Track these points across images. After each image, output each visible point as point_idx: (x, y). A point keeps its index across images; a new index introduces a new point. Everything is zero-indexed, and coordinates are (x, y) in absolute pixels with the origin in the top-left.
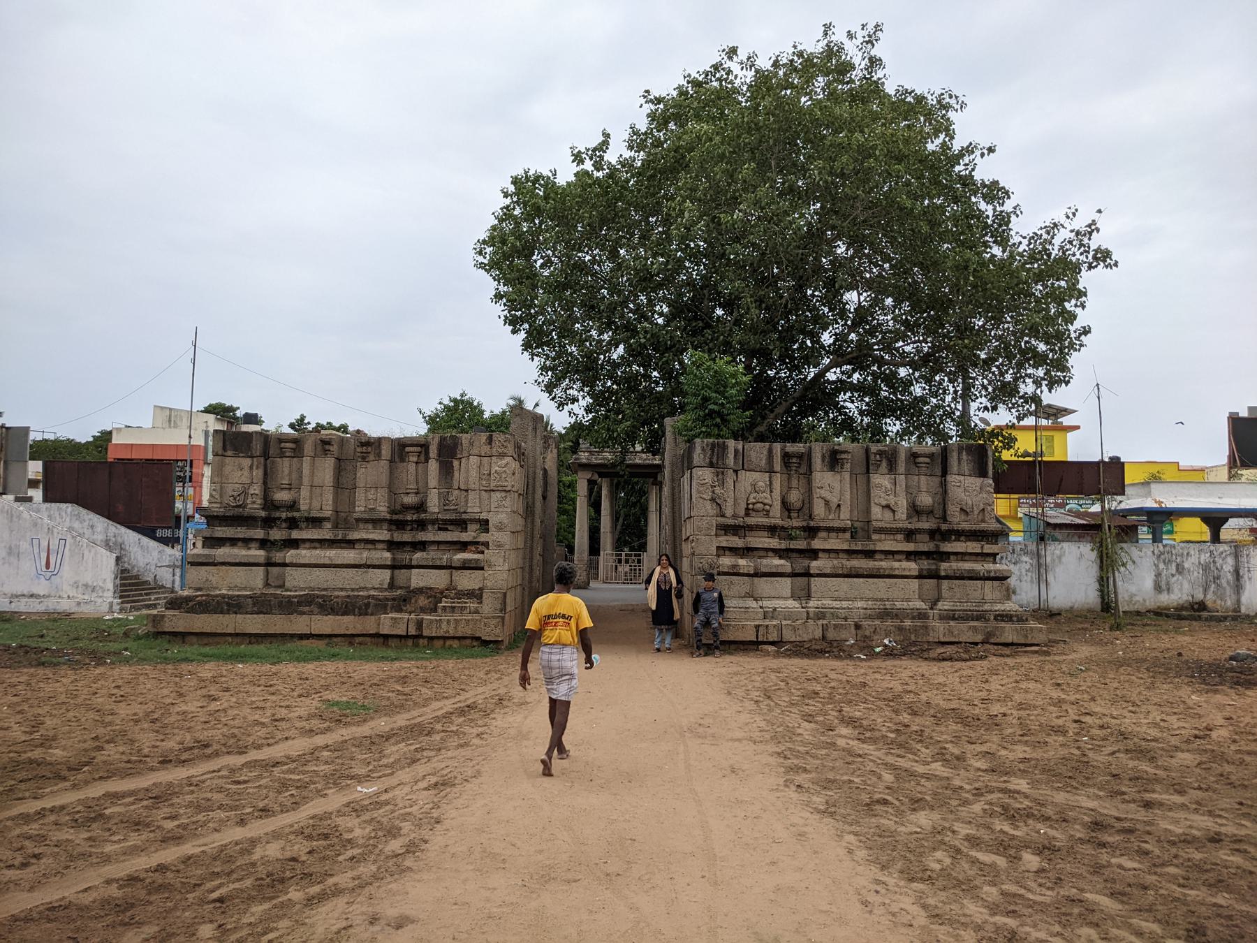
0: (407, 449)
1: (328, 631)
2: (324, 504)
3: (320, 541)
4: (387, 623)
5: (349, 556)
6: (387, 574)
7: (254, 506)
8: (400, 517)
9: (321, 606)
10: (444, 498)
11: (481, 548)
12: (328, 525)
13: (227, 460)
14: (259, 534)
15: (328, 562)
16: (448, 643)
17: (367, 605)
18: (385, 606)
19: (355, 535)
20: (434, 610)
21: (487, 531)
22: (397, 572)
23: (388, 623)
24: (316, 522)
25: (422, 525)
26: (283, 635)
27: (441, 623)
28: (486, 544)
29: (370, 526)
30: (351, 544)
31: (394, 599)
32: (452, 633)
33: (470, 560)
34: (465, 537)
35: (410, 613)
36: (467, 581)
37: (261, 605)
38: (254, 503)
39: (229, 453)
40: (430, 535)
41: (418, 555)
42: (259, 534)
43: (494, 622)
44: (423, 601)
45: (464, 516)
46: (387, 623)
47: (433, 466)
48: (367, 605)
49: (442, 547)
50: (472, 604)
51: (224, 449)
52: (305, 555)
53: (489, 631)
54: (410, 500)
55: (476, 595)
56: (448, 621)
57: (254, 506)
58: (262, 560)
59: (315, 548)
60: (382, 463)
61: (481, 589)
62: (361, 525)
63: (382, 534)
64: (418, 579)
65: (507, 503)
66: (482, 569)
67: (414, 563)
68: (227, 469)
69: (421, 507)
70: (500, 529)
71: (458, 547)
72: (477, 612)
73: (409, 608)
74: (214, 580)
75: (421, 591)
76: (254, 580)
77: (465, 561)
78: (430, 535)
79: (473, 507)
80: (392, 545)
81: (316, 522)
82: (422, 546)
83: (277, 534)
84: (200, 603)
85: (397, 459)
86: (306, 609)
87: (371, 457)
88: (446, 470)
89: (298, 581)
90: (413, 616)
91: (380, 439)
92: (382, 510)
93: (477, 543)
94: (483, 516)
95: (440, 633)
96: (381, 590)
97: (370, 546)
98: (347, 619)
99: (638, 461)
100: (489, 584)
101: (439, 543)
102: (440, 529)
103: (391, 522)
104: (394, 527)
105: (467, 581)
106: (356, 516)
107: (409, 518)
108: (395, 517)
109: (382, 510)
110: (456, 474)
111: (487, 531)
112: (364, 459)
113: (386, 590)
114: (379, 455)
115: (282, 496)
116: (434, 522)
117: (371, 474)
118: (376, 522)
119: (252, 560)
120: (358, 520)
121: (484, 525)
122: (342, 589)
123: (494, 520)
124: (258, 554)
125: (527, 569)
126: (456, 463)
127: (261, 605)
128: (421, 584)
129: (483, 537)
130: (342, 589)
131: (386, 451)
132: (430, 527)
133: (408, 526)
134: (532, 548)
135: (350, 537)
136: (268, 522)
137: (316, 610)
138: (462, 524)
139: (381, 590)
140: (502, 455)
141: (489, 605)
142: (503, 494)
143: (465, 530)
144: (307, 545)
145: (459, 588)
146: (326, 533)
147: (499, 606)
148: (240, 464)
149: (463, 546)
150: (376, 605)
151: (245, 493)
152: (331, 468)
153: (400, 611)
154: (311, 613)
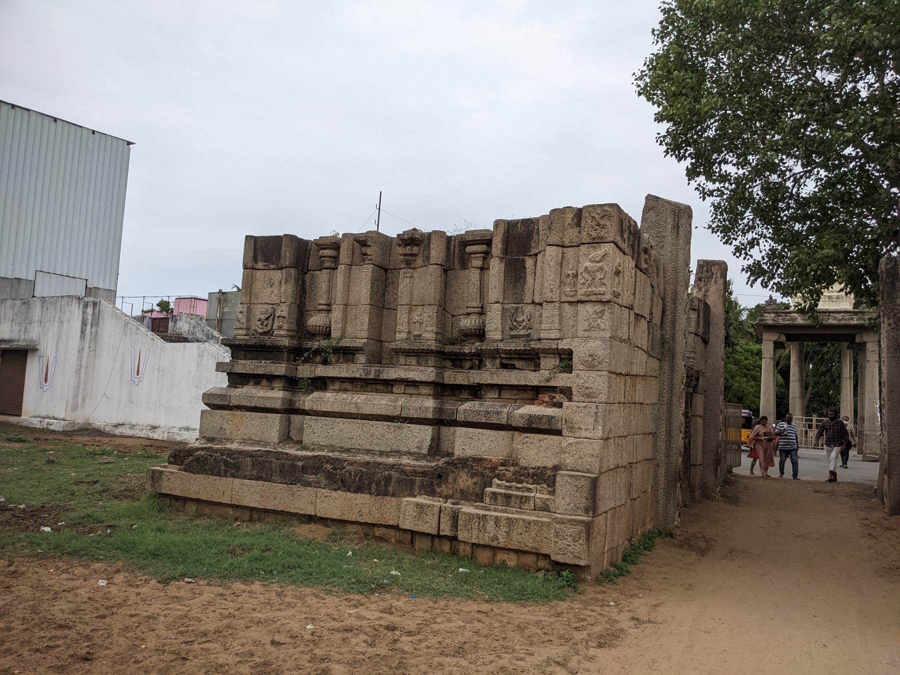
0: (469, 249)
1: (336, 515)
2: (357, 330)
3: (352, 380)
4: (411, 511)
5: (380, 403)
6: (426, 433)
7: (282, 337)
8: (456, 348)
9: (330, 476)
10: (510, 316)
11: (558, 397)
12: (361, 358)
13: (259, 274)
14: (280, 369)
15: (353, 410)
16: (501, 556)
17: (388, 479)
18: (411, 484)
19: (391, 374)
20: (480, 497)
21: (569, 369)
22: (445, 430)
23: (411, 511)
24: (347, 354)
25: (478, 360)
26: (282, 513)
27: (485, 521)
28: (567, 393)
29: (413, 361)
30: (388, 385)
31: (424, 474)
32: (502, 541)
33: (540, 418)
34: (533, 378)
35: (446, 498)
36: (535, 452)
37: (263, 466)
38: (280, 328)
39: (260, 265)
40: (489, 375)
41: (467, 405)
42: (280, 369)
43: (572, 530)
44: (464, 481)
45: (534, 345)
46: (411, 511)
47: (496, 267)
48: (388, 479)
49: (506, 394)
50: (539, 494)
51: (255, 260)
52: (329, 399)
53: (567, 547)
54: (468, 323)
55: (545, 477)
56: (497, 520)
57: (282, 337)
58: (278, 405)
59: (346, 390)
60: (432, 268)
61: (556, 468)
62: (402, 360)
63: (426, 373)
64: (465, 443)
65: (605, 322)
66: (559, 433)
67: (460, 417)
68: (258, 285)
69: (480, 334)
70: (591, 367)
71: (529, 395)
72: (545, 508)
73: (444, 489)
74: (228, 428)
75: (464, 463)
76: (268, 430)
77: (531, 418)
78: (489, 375)
79: (548, 328)
80: (441, 390)
81: (347, 354)
82: (476, 391)
83: (305, 371)
84: (197, 459)
85: (457, 265)
86: (311, 478)
87: (419, 261)
88: (516, 274)
89: (319, 435)
90: (448, 505)
91: (430, 234)
92: (429, 337)
93: (553, 389)
94: (563, 345)
95: (485, 539)
96: (418, 456)
97: (412, 390)
98: (362, 499)
99: (831, 321)
100: (569, 461)
101: (500, 388)
102: (504, 366)
103: (440, 354)
104: (448, 364)
105: (535, 452)
106: (393, 346)
107: (467, 350)
108: (449, 348)
109: (429, 337)
110: (530, 279)
111: (569, 369)
112: (408, 264)
113: (425, 457)
114: (428, 258)
115: (315, 320)
116: (494, 354)
117: (418, 285)
118: (420, 355)
119: (268, 405)
120: (398, 352)
121: (566, 359)
122: (368, 452)
123: (581, 350)
124: (276, 395)
125: (663, 436)
126: (529, 262)
127: (263, 466)
128: (469, 452)
129: (562, 380)
130: (368, 452)
131: (437, 252)
132: (488, 363)
133: (459, 366)
134: (670, 405)
135: (384, 376)
136: (297, 353)
137: (324, 481)
138: (532, 358)
139: (418, 456)
140: (596, 242)
141: (566, 499)
142: (598, 308)
143: (537, 368)
144: (337, 386)
145: (523, 463)
146: (355, 369)
147: (583, 503)
148: (270, 279)
149: (534, 393)
150: (399, 481)
151: (272, 316)
152: (369, 278)
153: (432, 493)
154: (317, 484)
